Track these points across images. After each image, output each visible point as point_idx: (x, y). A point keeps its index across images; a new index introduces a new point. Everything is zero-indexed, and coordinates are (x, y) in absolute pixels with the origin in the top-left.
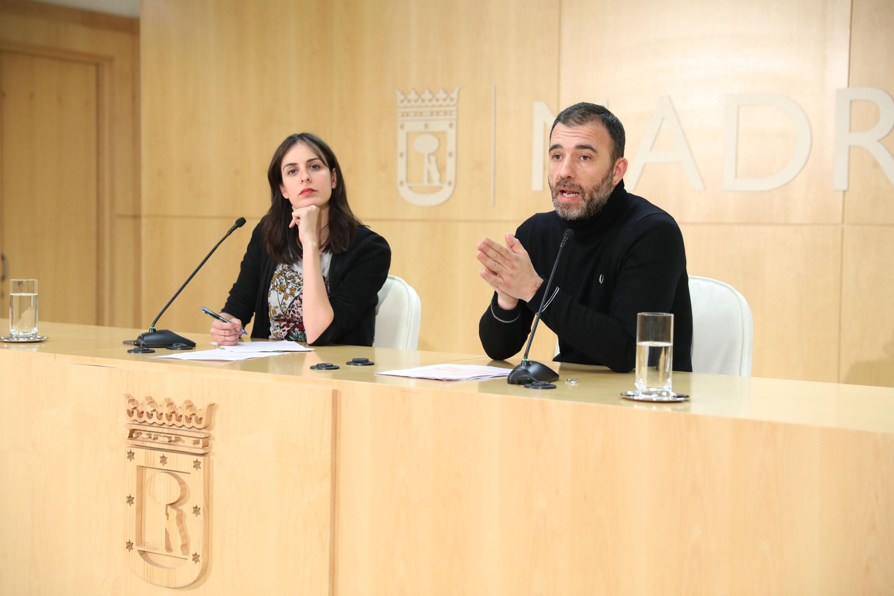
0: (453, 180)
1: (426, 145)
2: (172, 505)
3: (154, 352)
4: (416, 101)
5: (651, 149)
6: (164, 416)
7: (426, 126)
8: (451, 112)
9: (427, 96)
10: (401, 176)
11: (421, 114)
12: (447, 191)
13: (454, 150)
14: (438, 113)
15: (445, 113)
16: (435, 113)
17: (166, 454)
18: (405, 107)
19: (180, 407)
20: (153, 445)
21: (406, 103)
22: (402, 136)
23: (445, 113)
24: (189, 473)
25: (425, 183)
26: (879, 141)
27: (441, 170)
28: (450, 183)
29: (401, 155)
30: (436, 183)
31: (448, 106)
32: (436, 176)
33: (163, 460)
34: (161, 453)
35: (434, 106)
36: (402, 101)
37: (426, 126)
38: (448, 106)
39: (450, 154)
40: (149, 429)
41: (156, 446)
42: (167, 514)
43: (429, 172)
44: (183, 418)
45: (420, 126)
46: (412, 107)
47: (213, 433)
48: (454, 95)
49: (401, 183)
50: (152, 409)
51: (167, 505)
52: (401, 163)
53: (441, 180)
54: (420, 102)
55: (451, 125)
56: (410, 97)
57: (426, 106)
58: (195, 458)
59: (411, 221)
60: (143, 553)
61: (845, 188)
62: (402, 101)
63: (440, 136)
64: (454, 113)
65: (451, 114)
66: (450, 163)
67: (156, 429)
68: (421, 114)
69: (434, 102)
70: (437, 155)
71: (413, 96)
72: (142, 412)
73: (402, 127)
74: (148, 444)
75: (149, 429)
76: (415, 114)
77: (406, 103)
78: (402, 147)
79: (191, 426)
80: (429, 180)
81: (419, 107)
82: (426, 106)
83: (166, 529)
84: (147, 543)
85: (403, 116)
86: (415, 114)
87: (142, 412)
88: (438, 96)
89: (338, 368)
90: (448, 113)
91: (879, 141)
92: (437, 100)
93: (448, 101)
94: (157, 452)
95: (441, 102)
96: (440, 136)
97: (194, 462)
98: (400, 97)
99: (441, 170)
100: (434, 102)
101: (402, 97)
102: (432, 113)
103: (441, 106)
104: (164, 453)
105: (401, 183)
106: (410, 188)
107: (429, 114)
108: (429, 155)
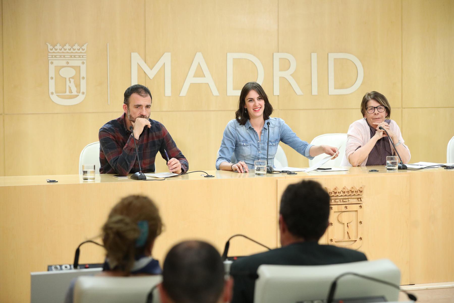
0: (85, 91)
1: (67, 73)
2: (349, 223)
3: (297, 174)
4: (61, 50)
5: (193, 77)
6: (346, 192)
7: (68, 63)
8: (83, 56)
9: (67, 47)
10: (52, 88)
11: (64, 56)
12: (81, 98)
13: (85, 76)
14: (75, 57)
15: (80, 56)
16: (73, 56)
17: (347, 206)
18: (54, 52)
19: (352, 188)
20: (341, 203)
21: (54, 50)
22: (52, 68)
23: (80, 56)
24: (357, 211)
25: (68, 93)
26: (291, 75)
27: (78, 86)
28: (83, 93)
29: (52, 78)
30: (75, 93)
31: (81, 53)
32: (74, 90)
33: (346, 207)
34: (345, 206)
35: (72, 52)
36: (52, 50)
37: (68, 63)
38: (81, 53)
39: (83, 78)
40: (339, 198)
41: (343, 203)
42: (348, 226)
43: (70, 88)
44: (354, 192)
45: (63, 63)
46: (58, 52)
47: (363, 195)
48: (84, 47)
49: (52, 93)
50: (340, 191)
51: (347, 223)
52: (52, 83)
53: (79, 92)
54: (63, 50)
55: (83, 63)
56: (56, 47)
57: (68, 52)
58: (360, 205)
59: (57, 113)
60: (335, 242)
61: (279, 95)
62: (52, 50)
63: (77, 69)
64: (84, 57)
65: (83, 57)
66: (83, 83)
67: (342, 198)
68: (64, 56)
69: (72, 50)
70: (77, 79)
71: (58, 47)
72: (336, 193)
73: (52, 63)
74: (339, 203)
75: (339, 198)
76: (61, 56)
77: (54, 50)
78: (52, 73)
79: (358, 194)
80: (71, 92)
81: (63, 53)
82: (68, 52)
83: (348, 233)
84: (335, 239)
85: (52, 57)
86: (61, 56)
87: (336, 193)
88: (74, 47)
89: (378, 171)
90: (81, 57)
91: (291, 75)
92: (74, 50)
93: (81, 50)
94: (343, 205)
95: (76, 51)
96: (77, 69)
97: (359, 206)
98: (50, 47)
99: (78, 86)
100: (72, 50)
101: (51, 47)
102: (71, 56)
103: (76, 52)
104: (346, 205)
105: (52, 93)
106: (57, 95)
107: (69, 56)
108: (70, 78)
